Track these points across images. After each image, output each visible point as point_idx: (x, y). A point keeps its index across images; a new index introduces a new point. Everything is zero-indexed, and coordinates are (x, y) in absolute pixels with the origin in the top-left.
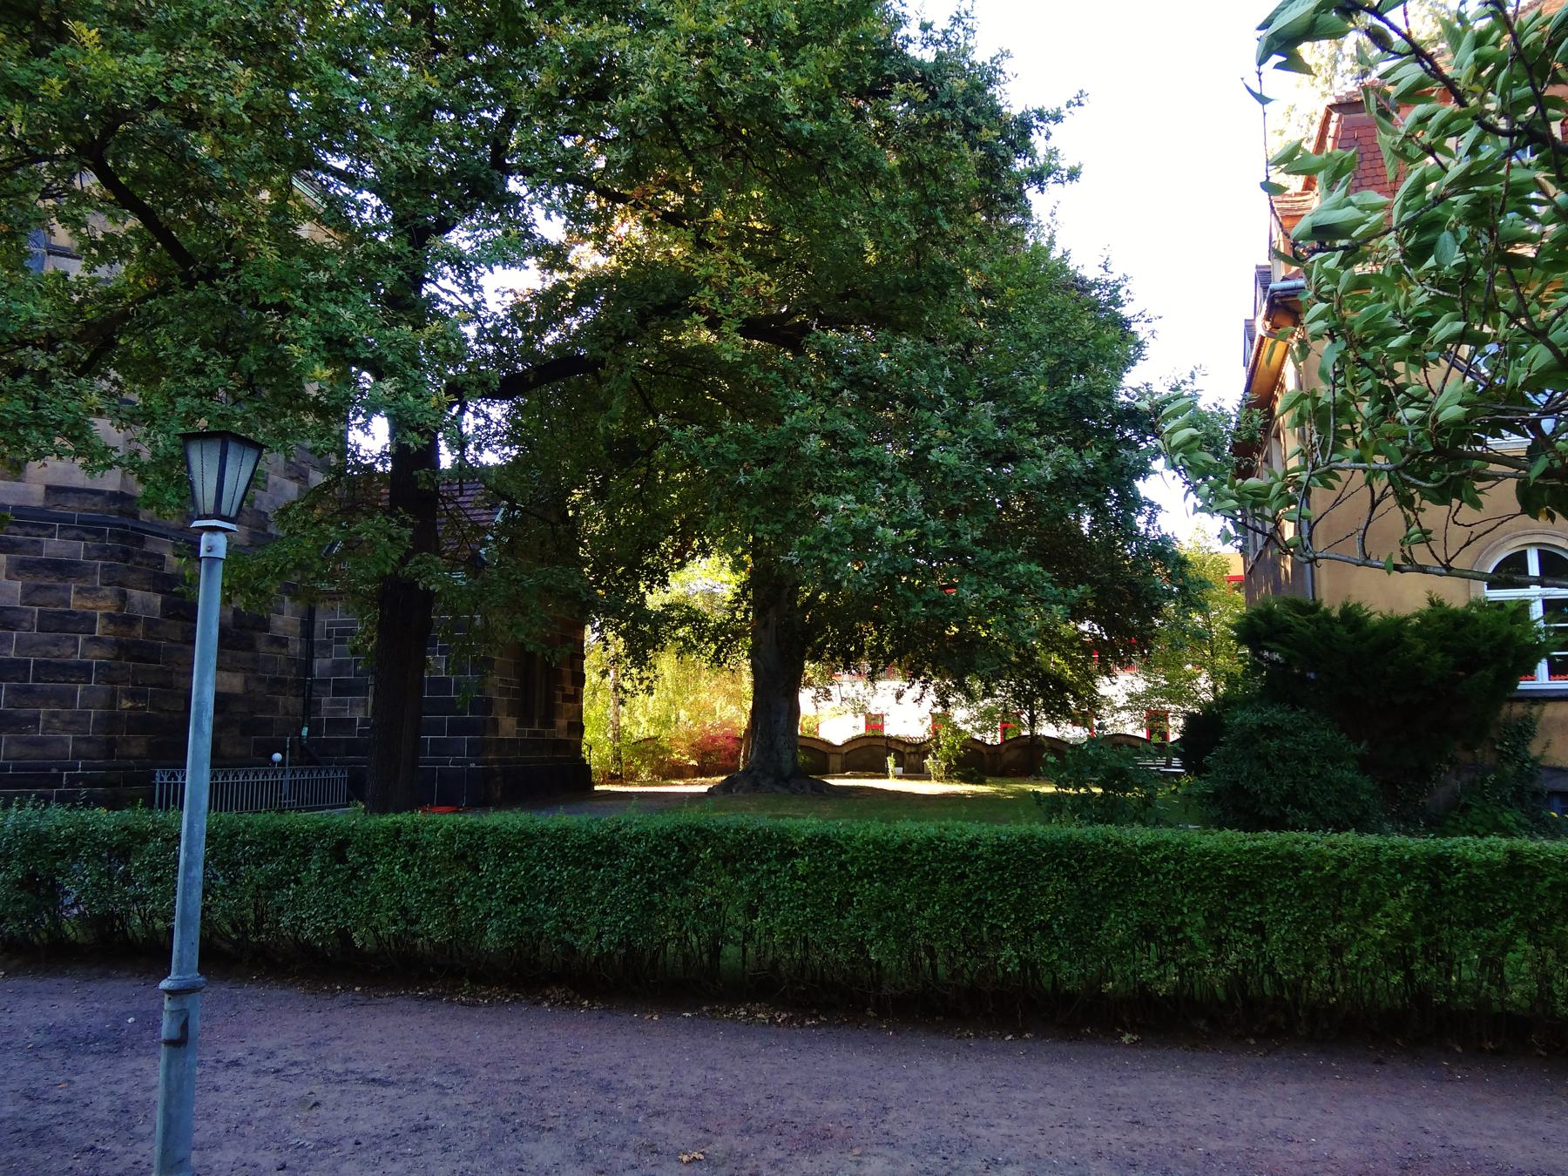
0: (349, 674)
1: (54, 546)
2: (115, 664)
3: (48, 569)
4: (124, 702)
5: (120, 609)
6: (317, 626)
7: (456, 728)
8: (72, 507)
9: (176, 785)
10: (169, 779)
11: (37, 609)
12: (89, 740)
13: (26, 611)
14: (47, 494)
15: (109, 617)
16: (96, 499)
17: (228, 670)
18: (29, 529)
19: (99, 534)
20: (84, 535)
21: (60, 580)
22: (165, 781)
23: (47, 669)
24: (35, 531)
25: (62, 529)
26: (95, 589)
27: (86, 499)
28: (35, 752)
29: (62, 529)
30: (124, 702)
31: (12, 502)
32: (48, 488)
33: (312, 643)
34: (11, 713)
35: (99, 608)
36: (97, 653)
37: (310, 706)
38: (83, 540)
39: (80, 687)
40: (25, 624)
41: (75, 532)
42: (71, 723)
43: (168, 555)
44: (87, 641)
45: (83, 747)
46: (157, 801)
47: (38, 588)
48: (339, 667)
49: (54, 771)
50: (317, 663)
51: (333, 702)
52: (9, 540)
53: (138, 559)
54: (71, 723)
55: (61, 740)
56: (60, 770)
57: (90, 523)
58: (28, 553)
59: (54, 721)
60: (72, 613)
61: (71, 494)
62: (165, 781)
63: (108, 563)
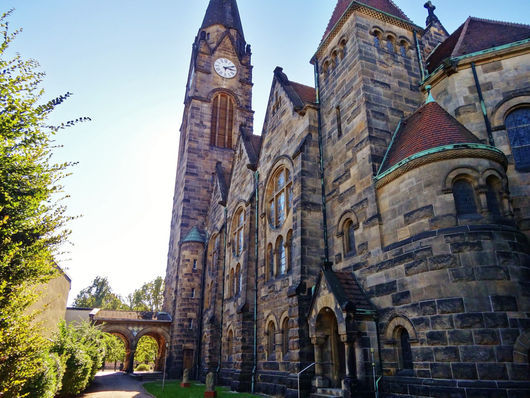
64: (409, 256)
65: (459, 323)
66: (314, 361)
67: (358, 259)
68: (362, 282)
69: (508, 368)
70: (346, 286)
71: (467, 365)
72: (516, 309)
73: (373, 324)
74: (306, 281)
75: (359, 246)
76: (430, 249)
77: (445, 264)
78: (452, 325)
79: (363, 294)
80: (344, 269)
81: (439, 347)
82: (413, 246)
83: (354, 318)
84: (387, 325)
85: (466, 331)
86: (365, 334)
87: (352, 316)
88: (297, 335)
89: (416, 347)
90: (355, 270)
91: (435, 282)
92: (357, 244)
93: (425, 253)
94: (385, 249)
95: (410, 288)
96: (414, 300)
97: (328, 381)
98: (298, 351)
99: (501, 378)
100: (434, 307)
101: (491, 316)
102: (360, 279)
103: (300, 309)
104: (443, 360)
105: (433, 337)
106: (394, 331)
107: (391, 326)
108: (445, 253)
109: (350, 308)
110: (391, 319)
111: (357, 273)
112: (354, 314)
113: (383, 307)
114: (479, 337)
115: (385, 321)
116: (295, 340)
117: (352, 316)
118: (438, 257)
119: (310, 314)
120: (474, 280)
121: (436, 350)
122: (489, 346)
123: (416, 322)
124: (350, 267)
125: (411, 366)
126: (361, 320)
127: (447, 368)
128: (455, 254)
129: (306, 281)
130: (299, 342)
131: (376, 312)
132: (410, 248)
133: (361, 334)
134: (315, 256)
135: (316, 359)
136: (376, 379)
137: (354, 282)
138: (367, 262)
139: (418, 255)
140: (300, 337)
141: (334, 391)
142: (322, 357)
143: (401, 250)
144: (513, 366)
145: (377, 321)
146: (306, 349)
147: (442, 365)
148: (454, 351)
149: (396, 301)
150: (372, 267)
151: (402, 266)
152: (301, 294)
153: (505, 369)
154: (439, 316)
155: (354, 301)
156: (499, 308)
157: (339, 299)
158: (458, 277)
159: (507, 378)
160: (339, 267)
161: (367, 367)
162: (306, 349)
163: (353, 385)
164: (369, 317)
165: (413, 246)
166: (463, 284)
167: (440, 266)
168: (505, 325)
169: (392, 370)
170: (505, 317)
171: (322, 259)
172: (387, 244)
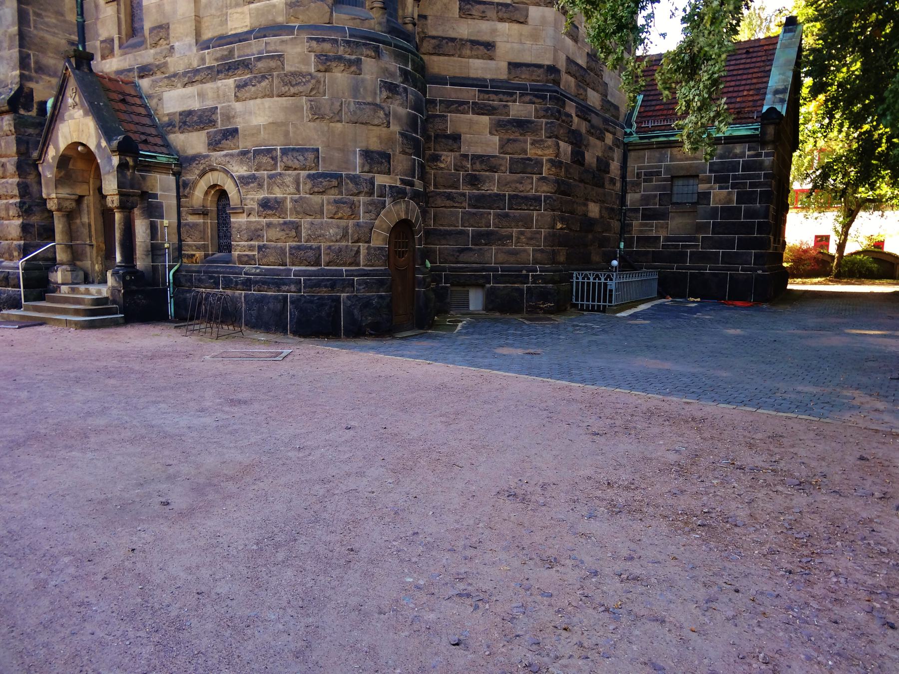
0: (656, 204)
1: (518, 109)
2: (555, 196)
3: (513, 126)
4: (558, 224)
5: (556, 157)
6: (629, 169)
7: (743, 244)
8: (525, 78)
9: (588, 283)
10: (594, 279)
11: (508, 156)
12: (542, 251)
13: (503, 158)
14: (509, 69)
15: (550, 161)
16: (541, 71)
17: (594, 202)
18: (501, 96)
19: (544, 98)
20: (535, 99)
21: (521, 135)
22: (591, 280)
23: (518, 200)
24: (505, 98)
25: (522, 95)
26: (542, 141)
27: (533, 71)
28: (512, 259)
29: (522, 95)
30: (558, 224)
31: (488, 76)
32: (510, 64)
33: (626, 182)
34: (497, 232)
35: (545, 155)
36: (545, 188)
37: (625, 228)
38: (534, 103)
39: (535, 213)
40: (503, 168)
41: (527, 98)
42: (531, 239)
43: (574, 115)
44: (539, 179)
45: (539, 256)
46: (574, 294)
47: (509, 140)
48: (646, 199)
49: (524, 272)
50: (629, 197)
51: (642, 225)
52: (490, 105)
53: (564, 118)
54: (531, 239)
55: (525, 251)
56: (528, 271)
57: (538, 90)
58: (501, 115)
59: (522, 237)
60: (529, 159)
61: (524, 68)
62: (580, 280)
63: (549, 121)
64: (245, 65)
65: (309, 186)
66: (54, 241)
67: (147, 56)
68: (152, 103)
69: (363, 252)
70: (122, 107)
71: (311, 248)
72: (389, 173)
73: (172, 178)
74: (31, 85)
75: (152, 30)
76: (280, 57)
77: (300, 88)
78: (298, 189)
79: (154, 126)
80: (120, 72)
81: (275, 220)
82: (254, 48)
83: (134, 168)
84: (195, 184)
85: (317, 199)
86: (155, 196)
87: (131, 163)
88: (16, 192)
89: (238, 220)
90: (142, 77)
91: (281, 117)
92: (147, 25)
93: (273, 64)
94: (204, 45)
95: (239, 123)
96: (245, 143)
97: (81, 275)
98: (18, 222)
99: (350, 265)
100: (274, 159)
101: (354, 179)
102: (150, 97)
103: (19, 142)
104: (277, 240)
105: (266, 205)
106: (206, 193)
107: (203, 185)
108: (303, 69)
109: (126, 148)
110: (203, 174)
111: (145, 84)
112: (135, 161)
113: (191, 152)
114: (332, 208)
115: (190, 177)
116: (11, 201)
117: (131, 163)
118: (293, 74)
119: (43, 152)
120: (340, 121)
121: (269, 225)
122: (343, 223)
123: (244, 181)
124: (130, 70)
125: (229, 248)
126: (149, 171)
127: (283, 250)
128: (320, 75)
129: (31, 85)
130: (21, 205)
131: (178, 160)
132: (248, 51)
133: (145, 195)
134: (54, 34)
135: (58, 236)
136: (171, 268)
137: (138, 101)
138: (165, 64)
139: (260, 65)
140: (21, 196)
141: (93, 288)
142: (71, 233)
143: (231, 51)
144: (368, 248)
145: (177, 174)
146: (35, 219)
147: (275, 248)
148: (297, 227)
149: (214, 144)
150: (175, 75)
151: (231, 82)
152: (22, 112)
153: (358, 252)
154: (280, 174)
155: (134, 137)
156: (366, 168)
157: (106, 129)
158: (317, 115)
159: (358, 264)
160: (108, 66)
161: (155, 250)
162: (35, 219)
163: (128, 278)
164: (164, 168)
165: (254, 48)
166: (324, 125)
167: (293, 90)
168: (371, 194)
169: (199, 254)
170: (372, 182)
171: (72, 43)
172: (207, 35)
